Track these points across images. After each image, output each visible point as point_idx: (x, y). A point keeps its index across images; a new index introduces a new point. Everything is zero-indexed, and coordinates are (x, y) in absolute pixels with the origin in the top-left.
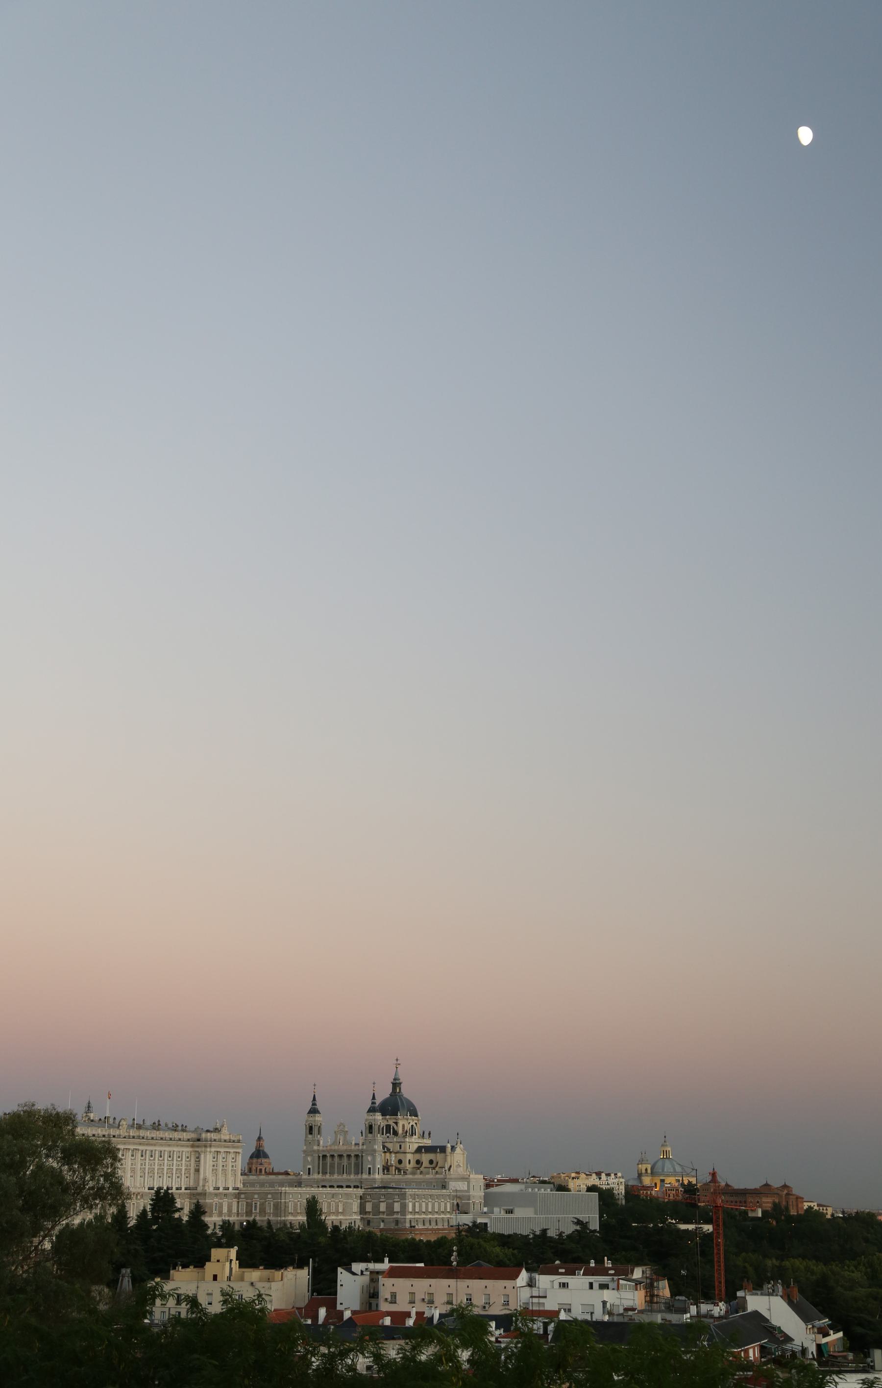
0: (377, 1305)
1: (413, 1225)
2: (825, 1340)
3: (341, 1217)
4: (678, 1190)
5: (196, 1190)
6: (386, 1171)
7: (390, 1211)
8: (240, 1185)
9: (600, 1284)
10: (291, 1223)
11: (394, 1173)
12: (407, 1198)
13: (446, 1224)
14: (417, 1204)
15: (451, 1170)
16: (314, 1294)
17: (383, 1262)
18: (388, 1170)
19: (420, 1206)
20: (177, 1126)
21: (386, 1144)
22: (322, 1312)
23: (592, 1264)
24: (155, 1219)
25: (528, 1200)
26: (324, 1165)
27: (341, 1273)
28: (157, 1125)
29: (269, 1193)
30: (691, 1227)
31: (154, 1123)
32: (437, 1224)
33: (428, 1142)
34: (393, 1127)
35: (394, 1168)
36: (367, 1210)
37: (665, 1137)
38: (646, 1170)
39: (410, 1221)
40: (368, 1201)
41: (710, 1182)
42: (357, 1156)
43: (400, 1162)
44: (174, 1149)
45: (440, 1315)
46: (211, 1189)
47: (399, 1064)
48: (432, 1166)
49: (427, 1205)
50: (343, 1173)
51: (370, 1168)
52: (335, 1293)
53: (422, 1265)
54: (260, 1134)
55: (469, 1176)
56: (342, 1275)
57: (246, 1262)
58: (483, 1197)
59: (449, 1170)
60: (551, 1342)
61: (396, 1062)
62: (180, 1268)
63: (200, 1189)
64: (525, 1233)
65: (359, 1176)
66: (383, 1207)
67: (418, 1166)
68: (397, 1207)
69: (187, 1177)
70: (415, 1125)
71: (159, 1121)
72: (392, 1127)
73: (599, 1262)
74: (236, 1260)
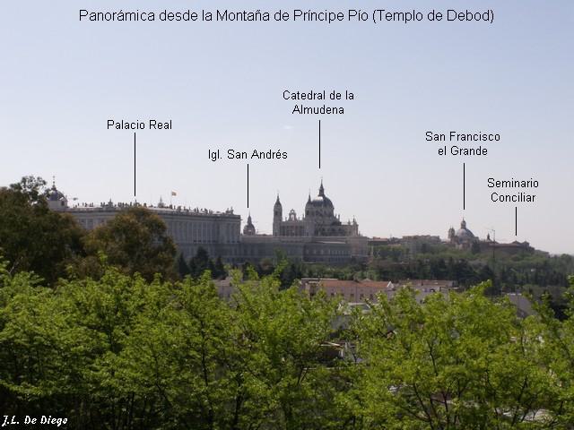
42: (301, 227)
66: (315, 252)
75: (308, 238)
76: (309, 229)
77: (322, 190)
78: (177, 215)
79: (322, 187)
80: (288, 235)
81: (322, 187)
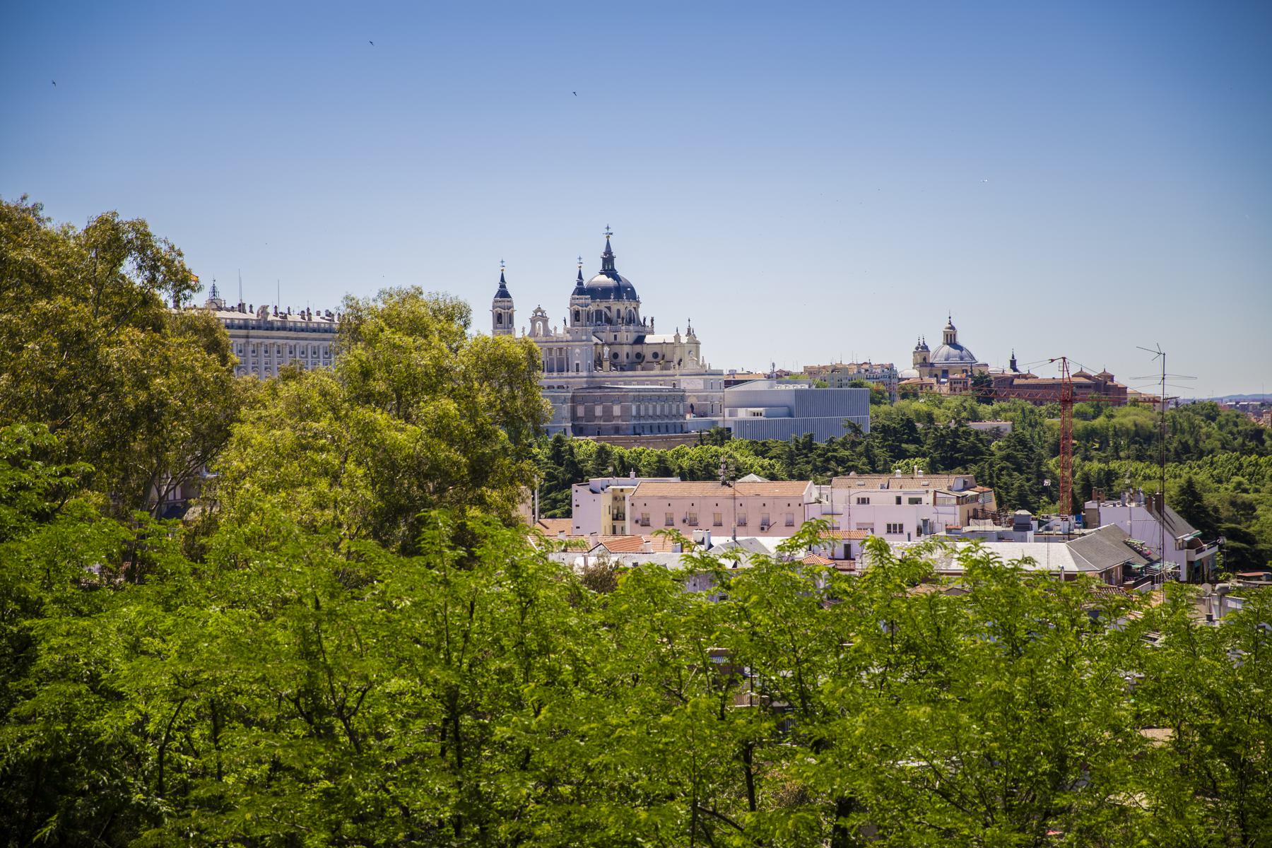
1: (638, 431)
2: (1198, 557)
14: (642, 408)
17: (628, 476)
18: (601, 366)
19: (647, 409)
36: (579, 415)
42: (561, 349)
43: (616, 356)
49: (655, 407)
51: (577, 365)
59: (679, 364)
65: (565, 374)
71: (308, 309)
75: (577, 379)
76: (579, 355)
77: (608, 259)
78: (257, 327)
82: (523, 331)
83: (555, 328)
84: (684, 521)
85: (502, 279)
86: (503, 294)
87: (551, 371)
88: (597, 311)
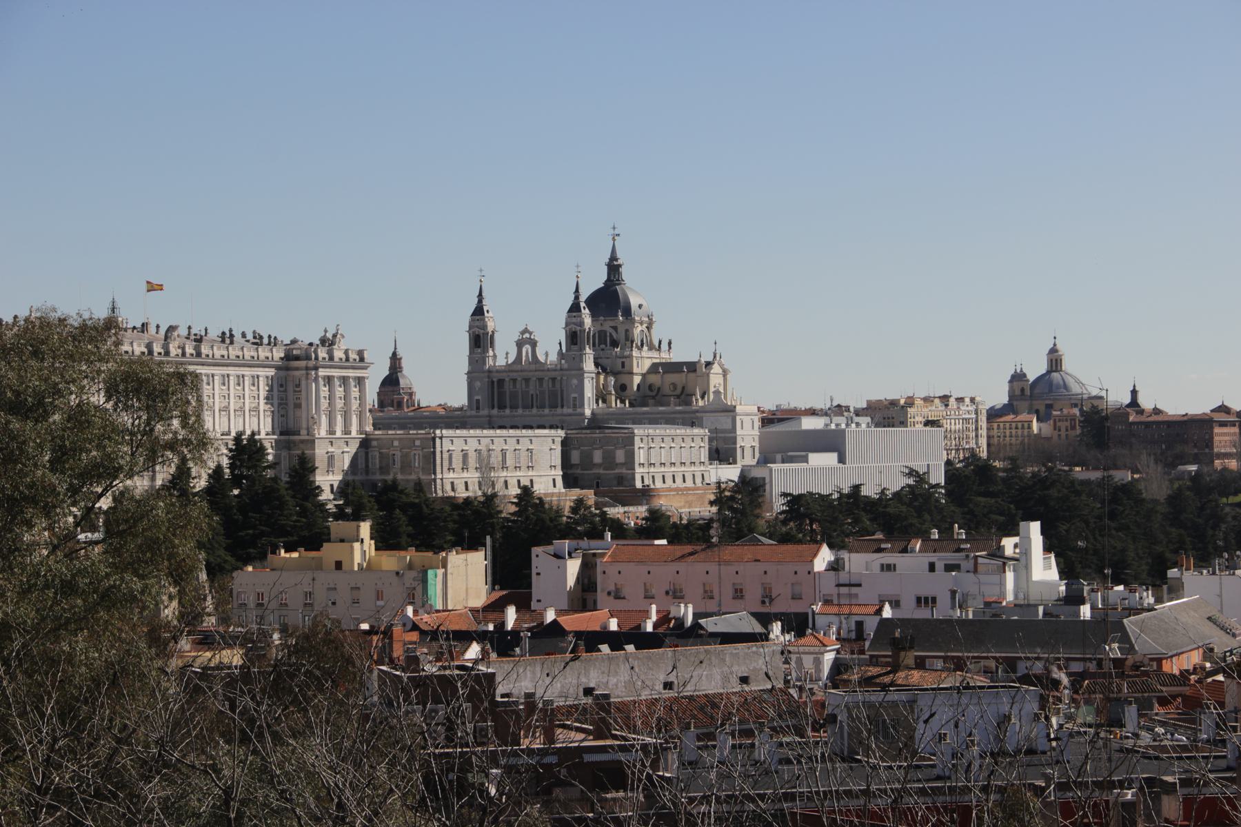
0: (595, 602)
1: (646, 482)
3: (530, 473)
4: (1074, 420)
5: (299, 435)
6: (600, 402)
7: (609, 461)
8: (369, 428)
9: (945, 565)
10: (452, 483)
11: (614, 405)
12: (636, 443)
13: (698, 480)
15: (706, 399)
16: (496, 587)
20: (261, 338)
21: (600, 361)
22: (511, 615)
23: (935, 534)
24: (236, 481)
25: (831, 442)
26: (501, 395)
27: (537, 556)
28: (228, 335)
29: (418, 439)
30: (1095, 475)
31: (224, 333)
32: (684, 481)
33: (665, 356)
34: (610, 334)
35: (613, 398)
37: (1055, 338)
38: (1023, 390)
39: (642, 477)
40: (575, 449)
41: (1128, 406)
42: (554, 379)
44: (259, 373)
45: (695, 614)
46: (323, 433)
47: (618, 235)
48: (675, 393)
50: (532, 407)
52: (529, 586)
53: (664, 542)
54: (395, 349)
55: (735, 407)
56: (540, 556)
57: (385, 540)
58: (757, 438)
59: (703, 397)
60: (868, 650)
61: (612, 232)
62: (283, 551)
63: (303, 436)
64: (825, 492)
65: (559, 411)
67: (654, 394)
68: (620, 456)
69: (282, 416)
70: (646, 330)
71: (231, 330)
72: (608, 334)
73: (946, 532)
74: (371, 538)
79: (613, 258)
80: (514, 407)
81: (613, 258)
82: (507, 358)
83: (547, 355)
84: (667, 593)
85: (480, 294)
86: (479, 312)
87: (542, 407)
88: (600, 332)
